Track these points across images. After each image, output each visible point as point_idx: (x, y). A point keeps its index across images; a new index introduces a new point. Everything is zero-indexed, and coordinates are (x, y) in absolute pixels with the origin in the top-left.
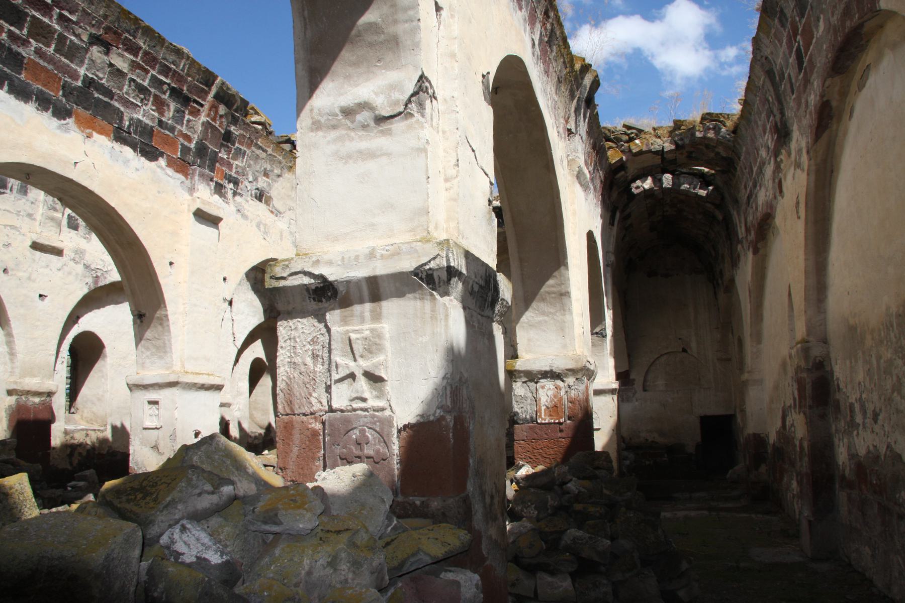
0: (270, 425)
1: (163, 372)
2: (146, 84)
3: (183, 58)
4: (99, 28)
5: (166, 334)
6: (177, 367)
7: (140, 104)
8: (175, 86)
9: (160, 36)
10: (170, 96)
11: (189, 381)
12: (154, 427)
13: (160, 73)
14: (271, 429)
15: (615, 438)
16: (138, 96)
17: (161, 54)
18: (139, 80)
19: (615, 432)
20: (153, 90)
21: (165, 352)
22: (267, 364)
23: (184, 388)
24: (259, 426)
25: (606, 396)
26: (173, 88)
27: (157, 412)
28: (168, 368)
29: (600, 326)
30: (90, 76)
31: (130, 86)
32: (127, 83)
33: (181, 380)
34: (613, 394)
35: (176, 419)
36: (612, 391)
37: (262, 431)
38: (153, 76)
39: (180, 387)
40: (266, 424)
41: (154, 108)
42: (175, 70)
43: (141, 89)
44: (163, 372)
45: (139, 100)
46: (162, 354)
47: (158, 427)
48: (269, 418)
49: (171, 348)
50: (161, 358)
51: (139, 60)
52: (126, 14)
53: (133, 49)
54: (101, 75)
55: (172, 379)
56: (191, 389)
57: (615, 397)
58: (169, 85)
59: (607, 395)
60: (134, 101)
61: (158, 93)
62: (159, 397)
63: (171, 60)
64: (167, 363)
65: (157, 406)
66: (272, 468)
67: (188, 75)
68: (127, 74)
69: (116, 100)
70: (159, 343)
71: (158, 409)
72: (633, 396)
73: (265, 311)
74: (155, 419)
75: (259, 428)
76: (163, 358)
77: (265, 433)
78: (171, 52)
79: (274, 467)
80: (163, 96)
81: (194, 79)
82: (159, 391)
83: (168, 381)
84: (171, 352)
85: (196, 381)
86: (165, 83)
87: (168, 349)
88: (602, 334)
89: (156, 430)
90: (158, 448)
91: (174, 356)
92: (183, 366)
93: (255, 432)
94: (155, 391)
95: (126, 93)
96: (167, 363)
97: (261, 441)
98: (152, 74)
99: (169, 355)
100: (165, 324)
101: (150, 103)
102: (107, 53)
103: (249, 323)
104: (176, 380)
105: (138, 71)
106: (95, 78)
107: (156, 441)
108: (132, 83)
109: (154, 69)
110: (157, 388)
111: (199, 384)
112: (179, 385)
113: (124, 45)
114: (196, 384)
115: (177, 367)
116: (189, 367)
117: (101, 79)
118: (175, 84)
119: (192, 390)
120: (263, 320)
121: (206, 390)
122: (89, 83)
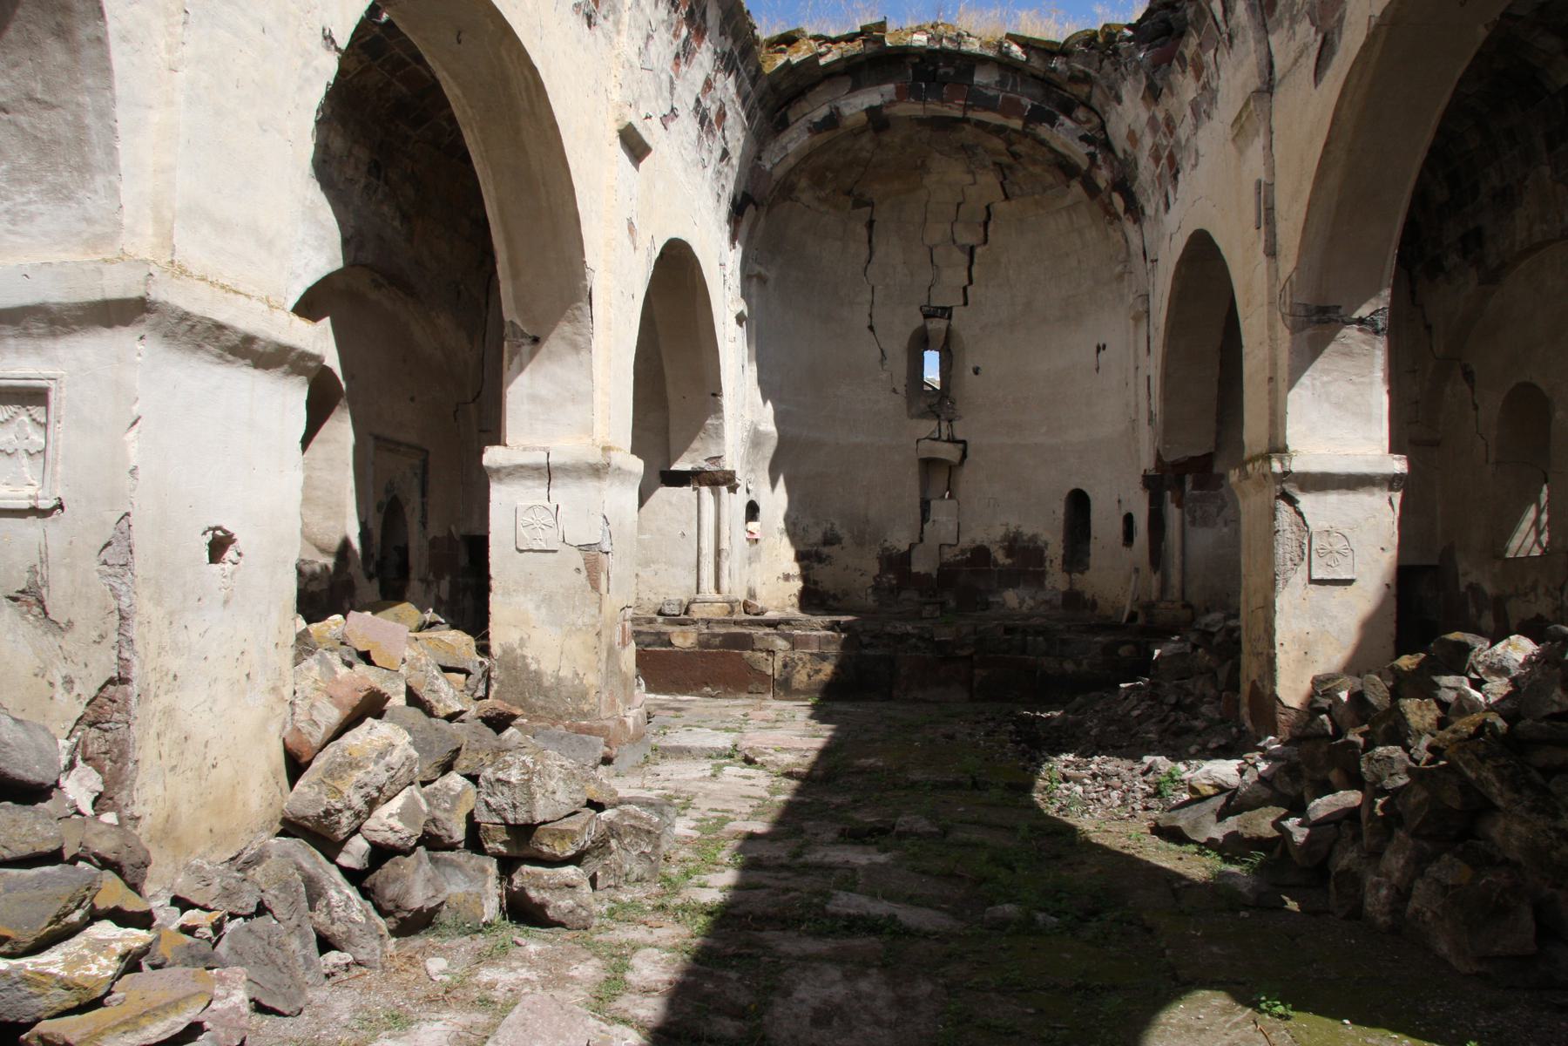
0: (346, 543)
1: (73, 255)
5: (89, 81)
6: (141, 241)
11: (196, 309)
12: (25, 504)
14: (349, 554)
15: (1392, 606)
19: (1393, 590)
21: (84, 169)
22: (344, 386)
23: (169, 336)
24: (317, 546)
25: (1374, 494)
27: (37, 438)
28: (95, 242)
29: (1373, 301)
33: (158, 294)
34: (1391, 489)
35: (133, 471)
36: (1391, 482)
37: (330, 561)
39: (155, 327)
40: (336, 542)
44: (73, 255)
46: (66, 176)
47: (45, 504)
48: (344, 526)
49: (111, 151)
50: (61, 194)
55: (117, 285)
56: (199, 346)
57: (1397, 497)
59: (1376, 490)
62: (49, 373)
64: (89, 221)
65: (38, 412)
66: (464, 676)
70: (53, 123)
71: (45, 426)
72: (1218, 516)
73: (346, 242)
74: (27, 468)
75: (316, 551)
76: (69, 198)
77: (336, 565)
79: (468, 673)
82: (48, 344)
83: (98, 297)
84: (113, 166)
85: (222, 317)
87: (99, 156)
88: (1373, 323)
89: (31, 519)
90: (41, 602)
91: (127, 192)
92: (167, 241)
93: (312, 562)
94: (28, 344)
96: (89, 221)
97: (325, 586)
99: (100, 180)
100: (84, 33)
103: (307, 265)
104: (134, 293)
107: (33, 570)
110: (42, 328)
111: (235, 331)
112: (151, 318)
114: (220, 327)
115: (141, 241)
116: (193, 250)
119: (200, 353)
120: (339, 264)
121: (256, 366)
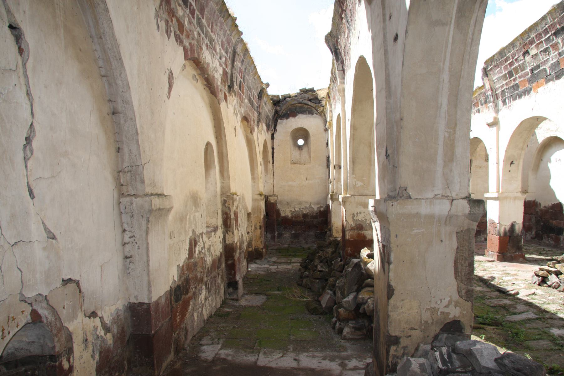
2: (545, 47)
3: (547, 17)
4: (522, 50)
7: (548, 57)
8: (554, 31)
9: (534, 24)
10: (556, 37)
13: (545, 35)
16: (546, 55)
17: (540, 29)
18: (542, 49)
20: (549, 46)
26: (554, 33)
30: (531, 68)
31: (542, 55)
32: (540, 55)
38: (546, 40)
41: (554, 51)
42: (549, 27)
43: (546, 50)
45: (547, 56)
51: (537, 42)
52: (522, 35)
53: (532, 42)
54: (532, 64)
58: (552, 35)
60: (546, 58)
61: (551, 44)
63: (544, 26)
67: (554, 19)
68: (538, 53)
69: (541, 66)
78: (541, 22)
80: (554, 42)
81: (558, 17)
86: (550, 36)
95: (543, 59)
98: (544, 40)
101: (551, 51)
102: (529, 54)
105: (539, 46)
106: (532, 67)
108: (541, 53)
109: (542, 38)
113: (530, 44)
117: (533, 65)
118: (553, 31)
122: (532, 70)
